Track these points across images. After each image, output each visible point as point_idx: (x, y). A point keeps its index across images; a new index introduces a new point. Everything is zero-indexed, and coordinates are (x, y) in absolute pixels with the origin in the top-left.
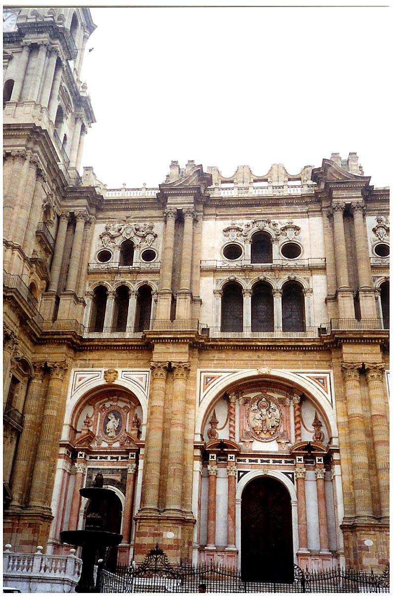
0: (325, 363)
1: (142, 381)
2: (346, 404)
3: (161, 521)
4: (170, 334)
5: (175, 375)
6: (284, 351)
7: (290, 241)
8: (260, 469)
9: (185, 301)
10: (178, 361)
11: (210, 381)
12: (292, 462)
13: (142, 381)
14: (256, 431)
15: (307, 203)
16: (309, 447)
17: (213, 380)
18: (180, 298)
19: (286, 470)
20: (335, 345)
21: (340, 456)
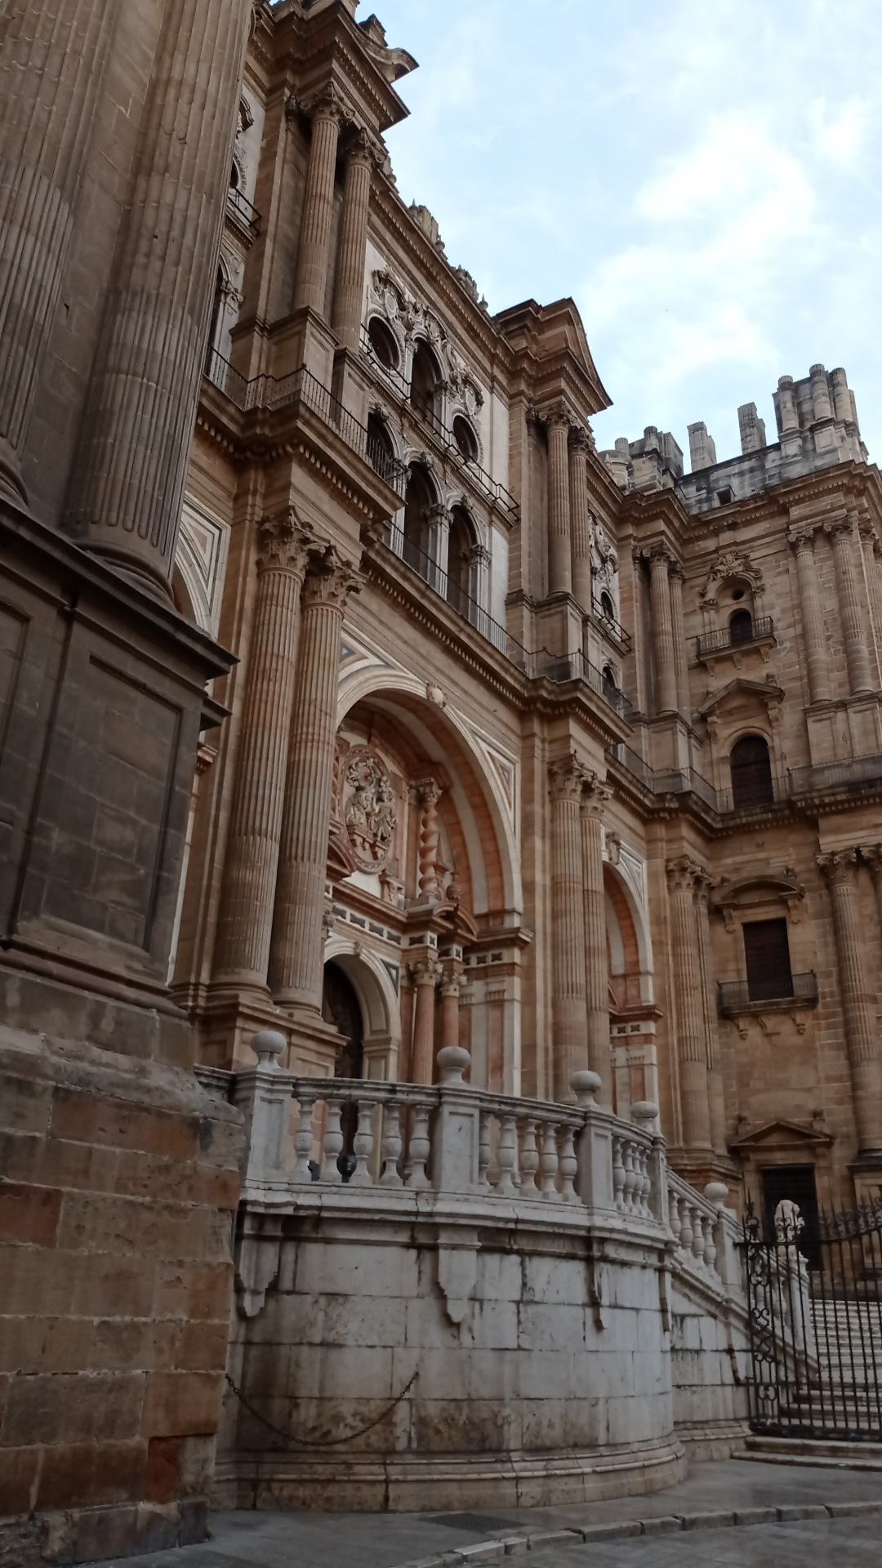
0: (513, 737)
1: (204, 545)
2: (553, 848)
3: (295, 1039)
4: (348, 462)
5: (324, 594)
6: (468, 670)
7: (468, 416)
8: (347, 937)
9: (358, 394)
10: (344, 559)
11: (347, 655)
12: (397, 940)
13: (204, 545)
14: (355, 837)
15: (493, 358)
16: (449, 916)
17: (352, 658)
18: (350, 375)
19: (389, 956)
20: (549, 710)
21: (532, 959)
